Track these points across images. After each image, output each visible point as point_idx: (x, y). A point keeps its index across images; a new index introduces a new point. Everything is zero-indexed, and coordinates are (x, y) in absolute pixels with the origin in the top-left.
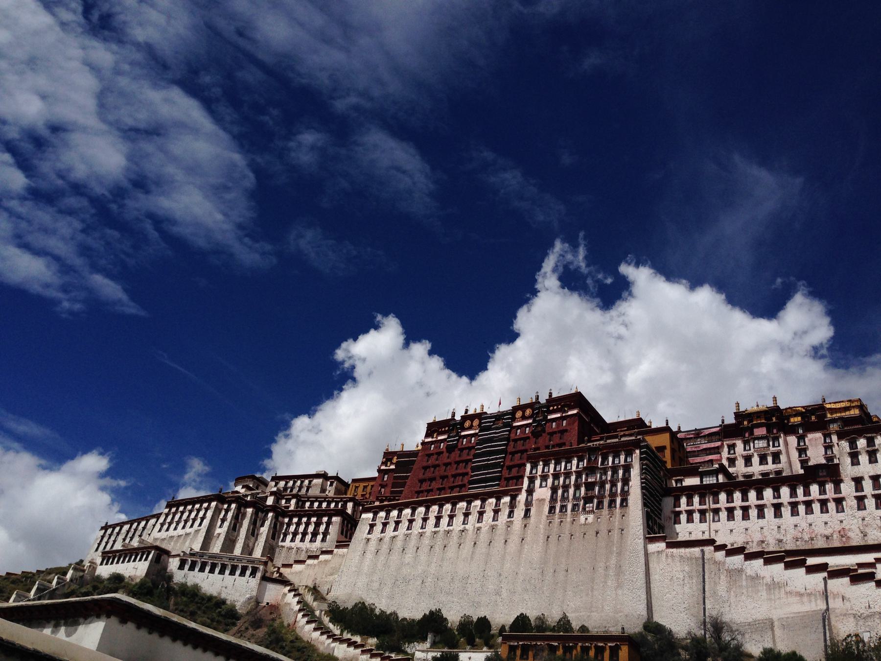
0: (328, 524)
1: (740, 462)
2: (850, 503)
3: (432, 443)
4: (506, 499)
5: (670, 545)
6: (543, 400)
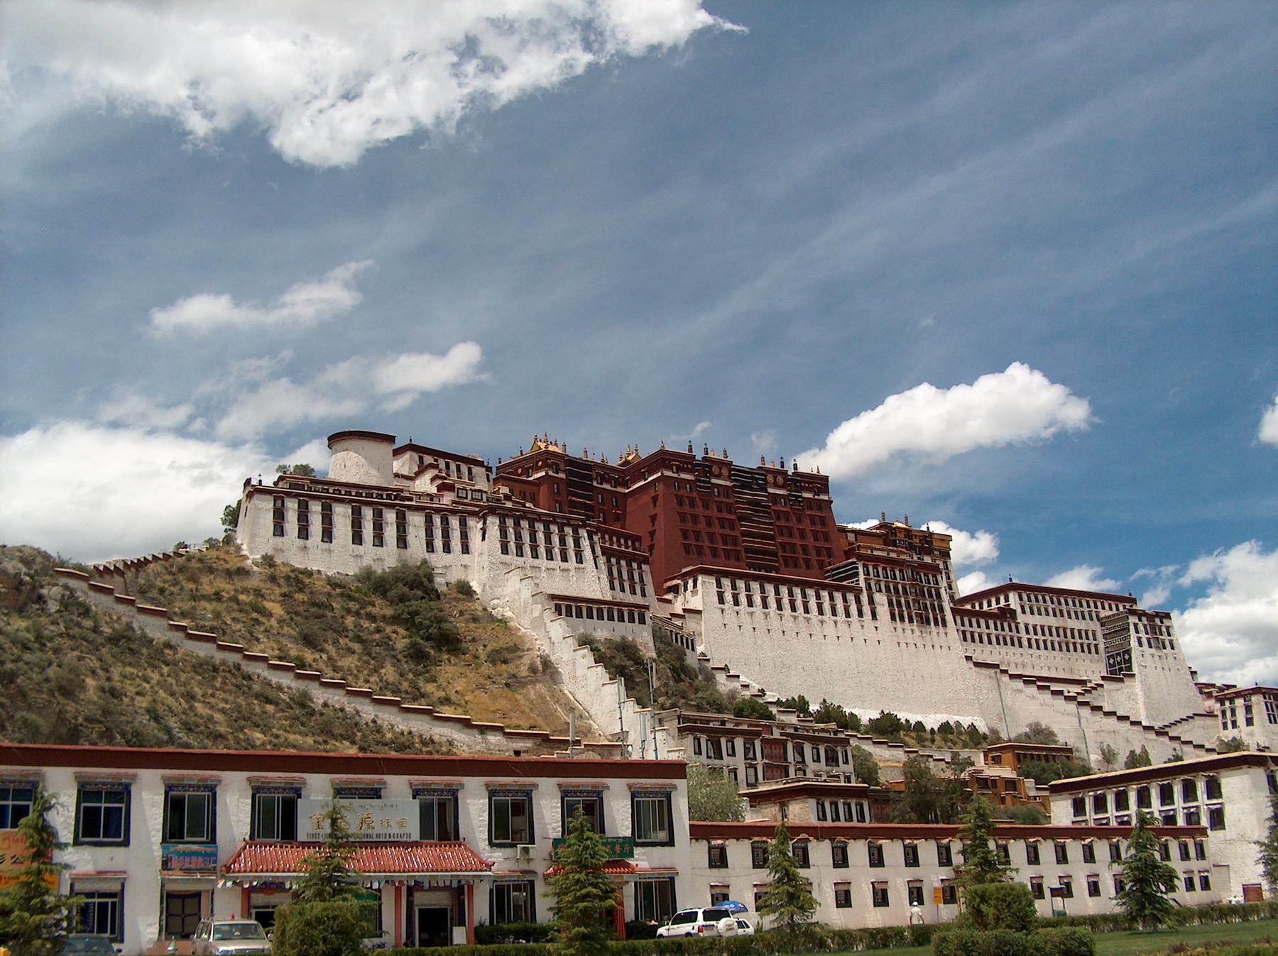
2: (1025, 643)
4: (851, 597)
5: (977, 664)
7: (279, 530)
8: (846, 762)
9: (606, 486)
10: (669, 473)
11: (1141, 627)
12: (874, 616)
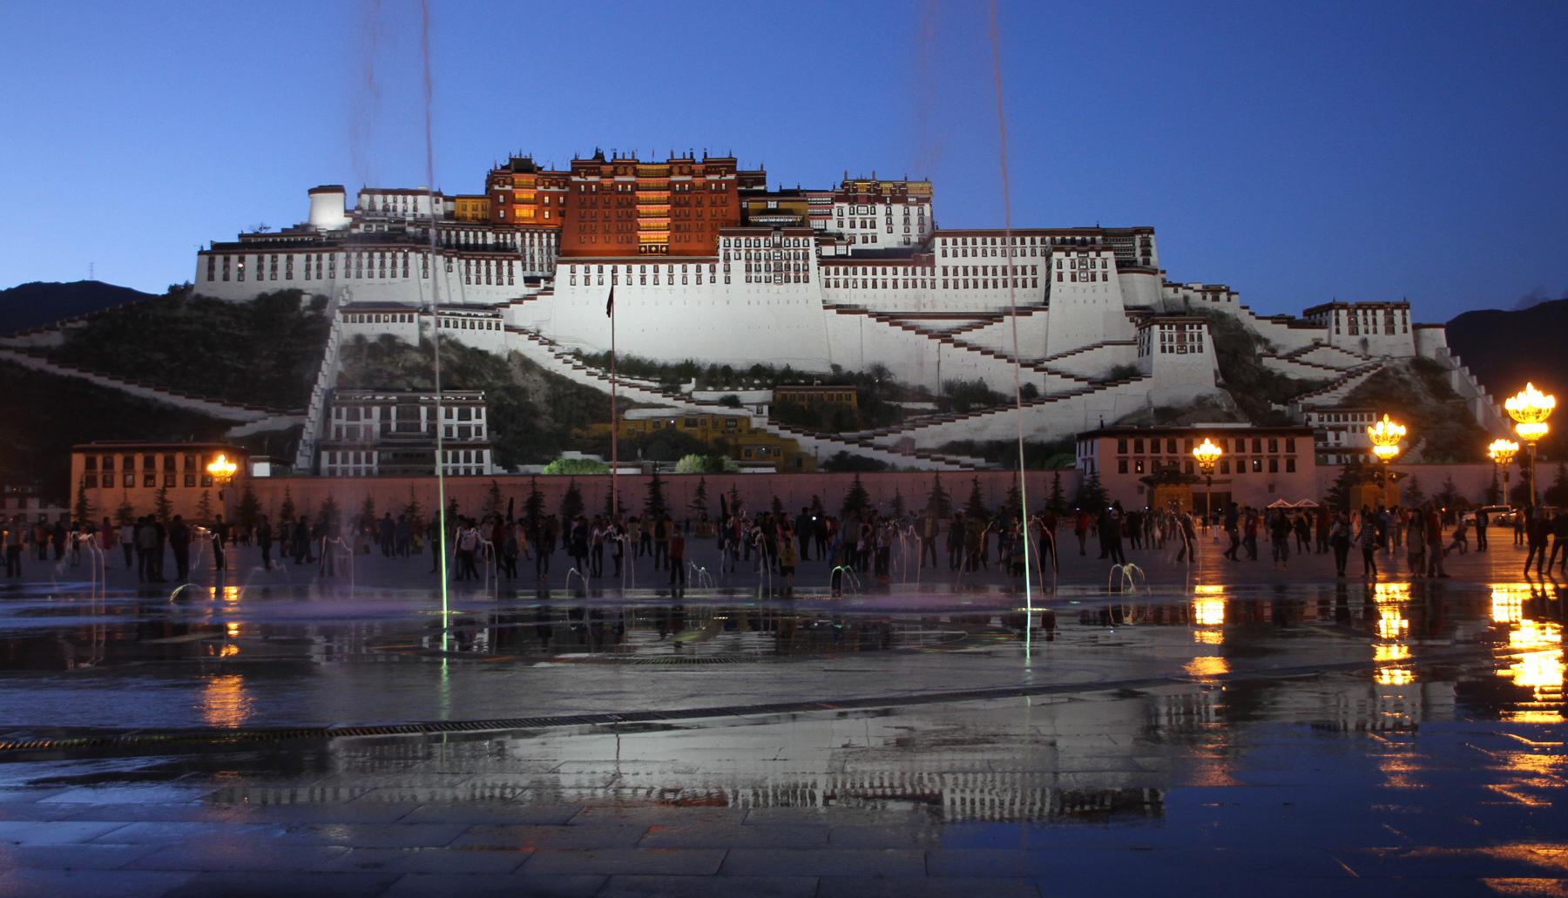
0: (510, 265)
1: (847, 223)
2: (939, 283)
3: (579, 183)
4: (705, 267)
6: (699, 158)
7: (211, 277)
8: (478, 416)
9: (553, 189)
10: (575, 179)
11: (1066, 262)
12: (728, 281)
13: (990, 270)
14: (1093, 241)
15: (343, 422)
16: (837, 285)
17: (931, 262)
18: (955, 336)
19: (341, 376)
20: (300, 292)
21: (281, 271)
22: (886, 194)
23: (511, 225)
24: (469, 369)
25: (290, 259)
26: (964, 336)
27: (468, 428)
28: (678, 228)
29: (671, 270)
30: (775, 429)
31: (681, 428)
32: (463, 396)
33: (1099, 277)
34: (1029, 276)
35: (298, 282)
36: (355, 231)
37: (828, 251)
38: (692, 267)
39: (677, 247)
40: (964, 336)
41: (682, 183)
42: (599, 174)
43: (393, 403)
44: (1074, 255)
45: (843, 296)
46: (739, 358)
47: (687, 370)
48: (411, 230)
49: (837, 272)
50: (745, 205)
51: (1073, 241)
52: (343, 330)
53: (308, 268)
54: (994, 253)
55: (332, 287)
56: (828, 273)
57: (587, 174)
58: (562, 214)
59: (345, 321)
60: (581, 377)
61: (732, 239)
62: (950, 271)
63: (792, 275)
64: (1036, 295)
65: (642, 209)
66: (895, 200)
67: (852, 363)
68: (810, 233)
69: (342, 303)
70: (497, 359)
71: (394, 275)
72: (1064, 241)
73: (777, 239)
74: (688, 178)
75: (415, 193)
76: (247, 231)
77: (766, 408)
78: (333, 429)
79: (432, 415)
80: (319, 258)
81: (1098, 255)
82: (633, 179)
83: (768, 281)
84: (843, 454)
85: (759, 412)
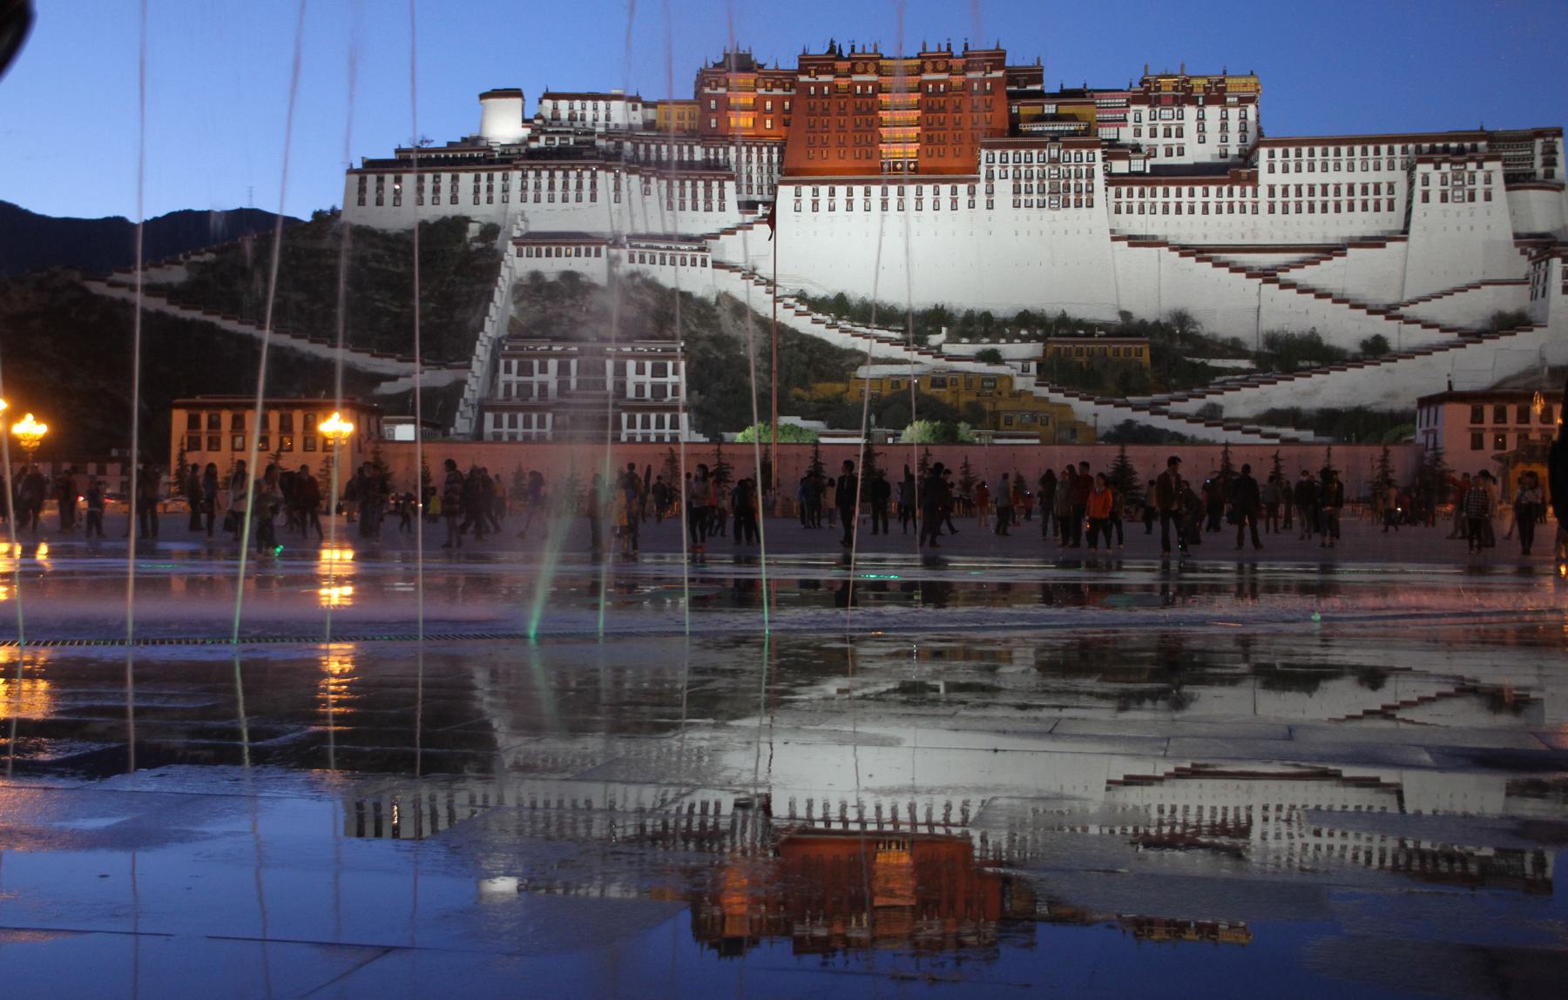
0: (721, 186)
1: (1146, 131)
2: (1263, 207)
3: (809, 84)
4: (962, 189)
6: (958, 50)
7: (362, 202)
8: (675, 372)
10: (803, 79)
11: (1435, 177)
12: (990, 205)
13: (1331, 189)
14: (1474, 149)
15: (513, 377)
16: (1130, 211)
17: (1253, 179)
18: (1282, 275)
19: (512, 321)
20: (467, 220)
21: (445, 193)
22: (1199, 92)
23: (725, 137)
24: (666, 314)
25: (455, 179)
26: (1294, 275)
27: (664, 387)
28: (930, 140)
29: (919, 193)
30: (1043, 392)
31: (928, 390)
32: (658, 347)
33: (1480, 195)
34: (1384, 196)
35: (465, 207)
36: (533, 145)
37: (1120, 167)
38: (945, 189)
39: (926, 163)
40: (1294, 275)
41: (936, 83)
42: (833, 72)
43: (572, 355)
44: (1446, 167)
45: (1137, 224)
46: (1003, 304)
47: (937, 318)
48: (601, 143)
49: (1130, 194)
50: (1015, 110)
51: (1446, 150)
52: (516, 266)
53: (477, 191)
54: (1338, 167)
55: (505, 214)
56: (1118, 195)
57: (818, 72)
58: (786, 124)
59: (520, 254)
60: (804, 325)
61: (997, 153)
62: (1278, 191)
63: (1072, 197)
64: (1393, 221)
65: (885, 116)
66: (1209, 101)
67: (1146, 309)
68: (1096, 145)
69: (517, 234)
70: (702, 302)
71: (579, 199)
72: (1433, 150)
73: (1054, 153)
74: (944, 76)
75: (608, 98)
76: (405, 146)
77: (1033, 365)
78: (501, 386)
79: (621, 370)
80: (490, 178)
81: (1480, 166)
82: (874, 78)
83: (1041, 206)
84: (1129, 423)
85: (1025, 370)
